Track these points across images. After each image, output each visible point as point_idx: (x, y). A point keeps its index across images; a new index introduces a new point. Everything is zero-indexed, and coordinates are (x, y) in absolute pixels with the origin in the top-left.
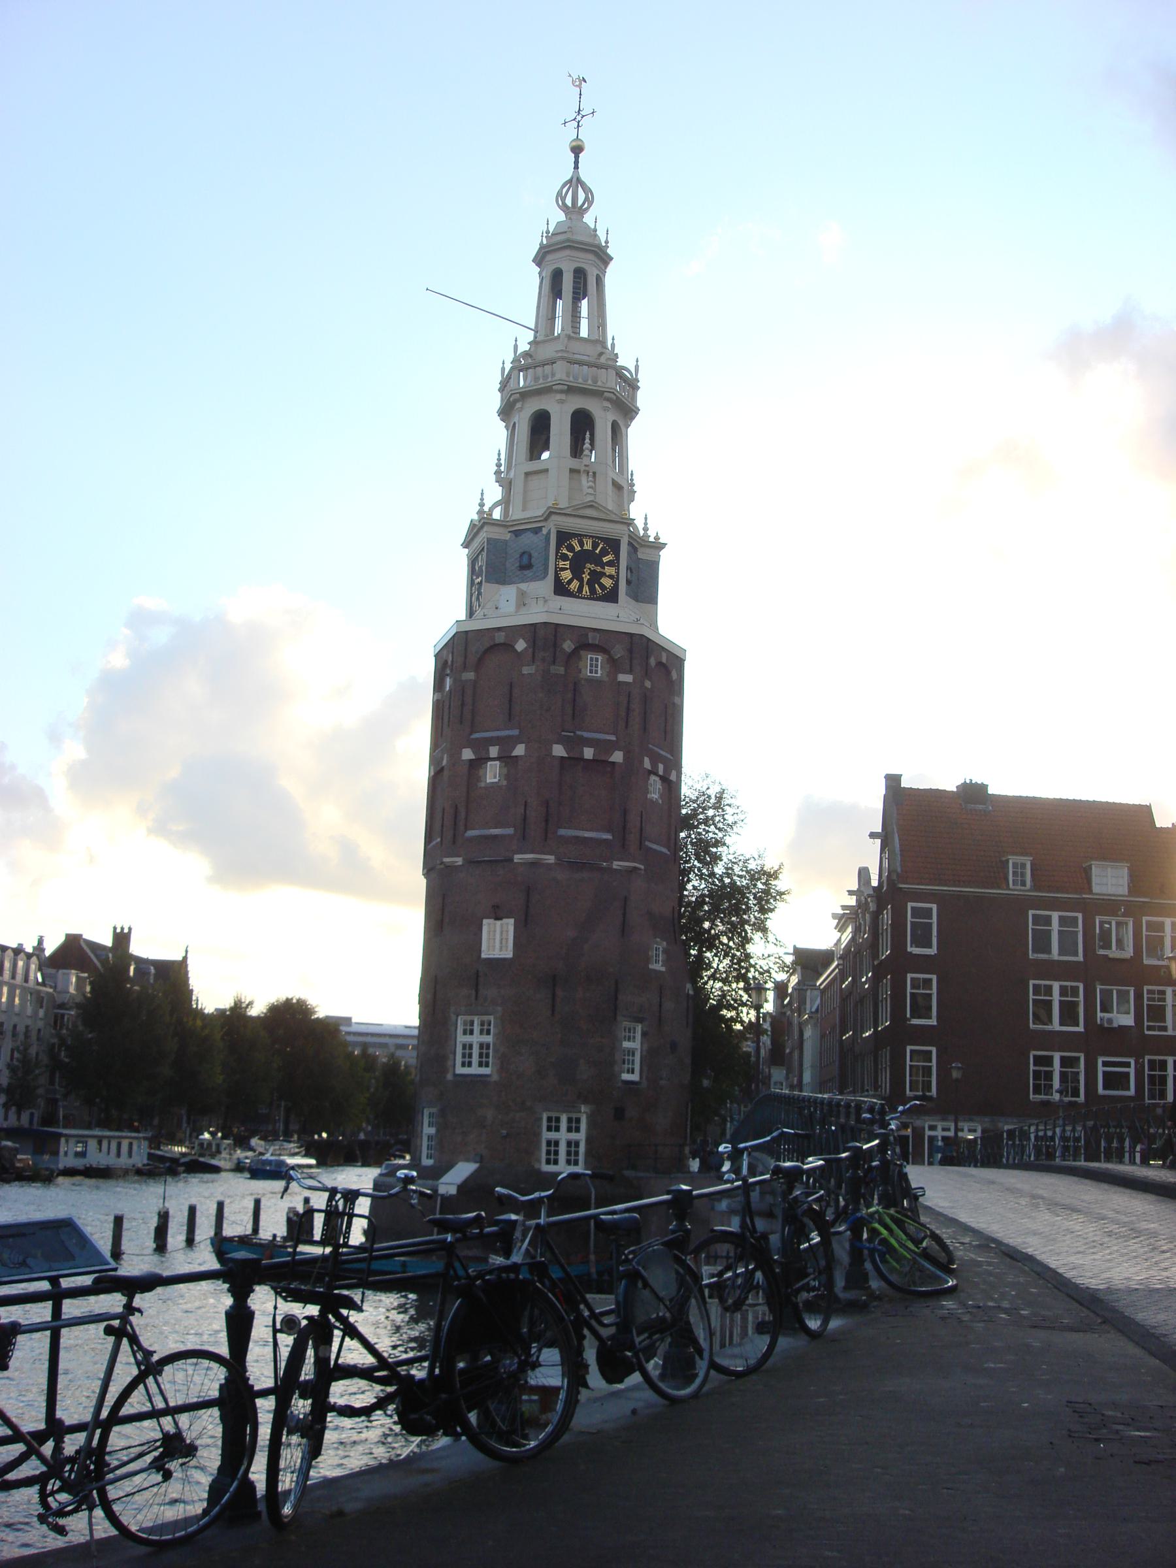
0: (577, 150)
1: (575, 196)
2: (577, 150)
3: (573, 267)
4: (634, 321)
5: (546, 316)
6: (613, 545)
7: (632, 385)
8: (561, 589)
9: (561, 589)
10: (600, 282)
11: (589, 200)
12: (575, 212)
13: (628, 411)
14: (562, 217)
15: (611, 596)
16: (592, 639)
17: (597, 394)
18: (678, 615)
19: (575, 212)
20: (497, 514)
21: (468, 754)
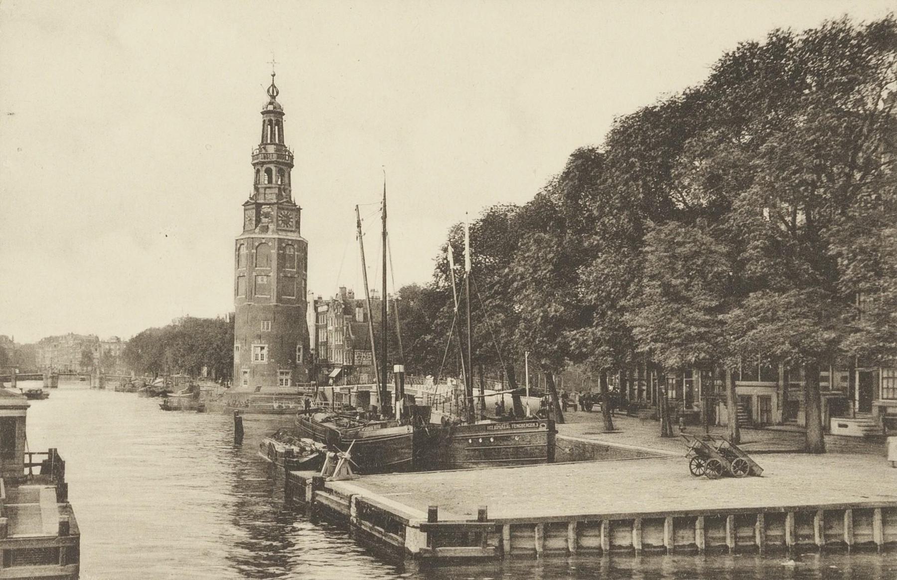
1: (273, 92)
2: (274, 75)
3: (274, 117)
7: (292, 158)
11: (277, 93)
12: (273, 97)
13: (291, 166)
14: (268, 99)
16: (290, 242)
19: (273, 97)
21: (254, 274)
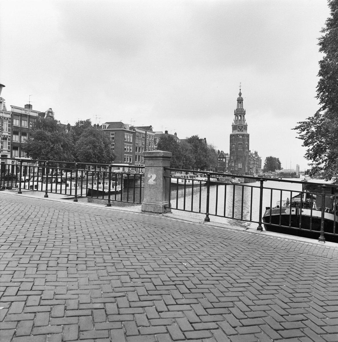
0: (240, 90)
1: (240, 94)
2: (240, 90)
4: (245, 106)
5: (238, 106)
6: (243, 127)
7: (245, 112)
8: (238, 131)
9: (238, 131)
10: (242, 102)
15: (242, 131)
17: (242, 114)
18: (249, 132)
20: (234, 124)
